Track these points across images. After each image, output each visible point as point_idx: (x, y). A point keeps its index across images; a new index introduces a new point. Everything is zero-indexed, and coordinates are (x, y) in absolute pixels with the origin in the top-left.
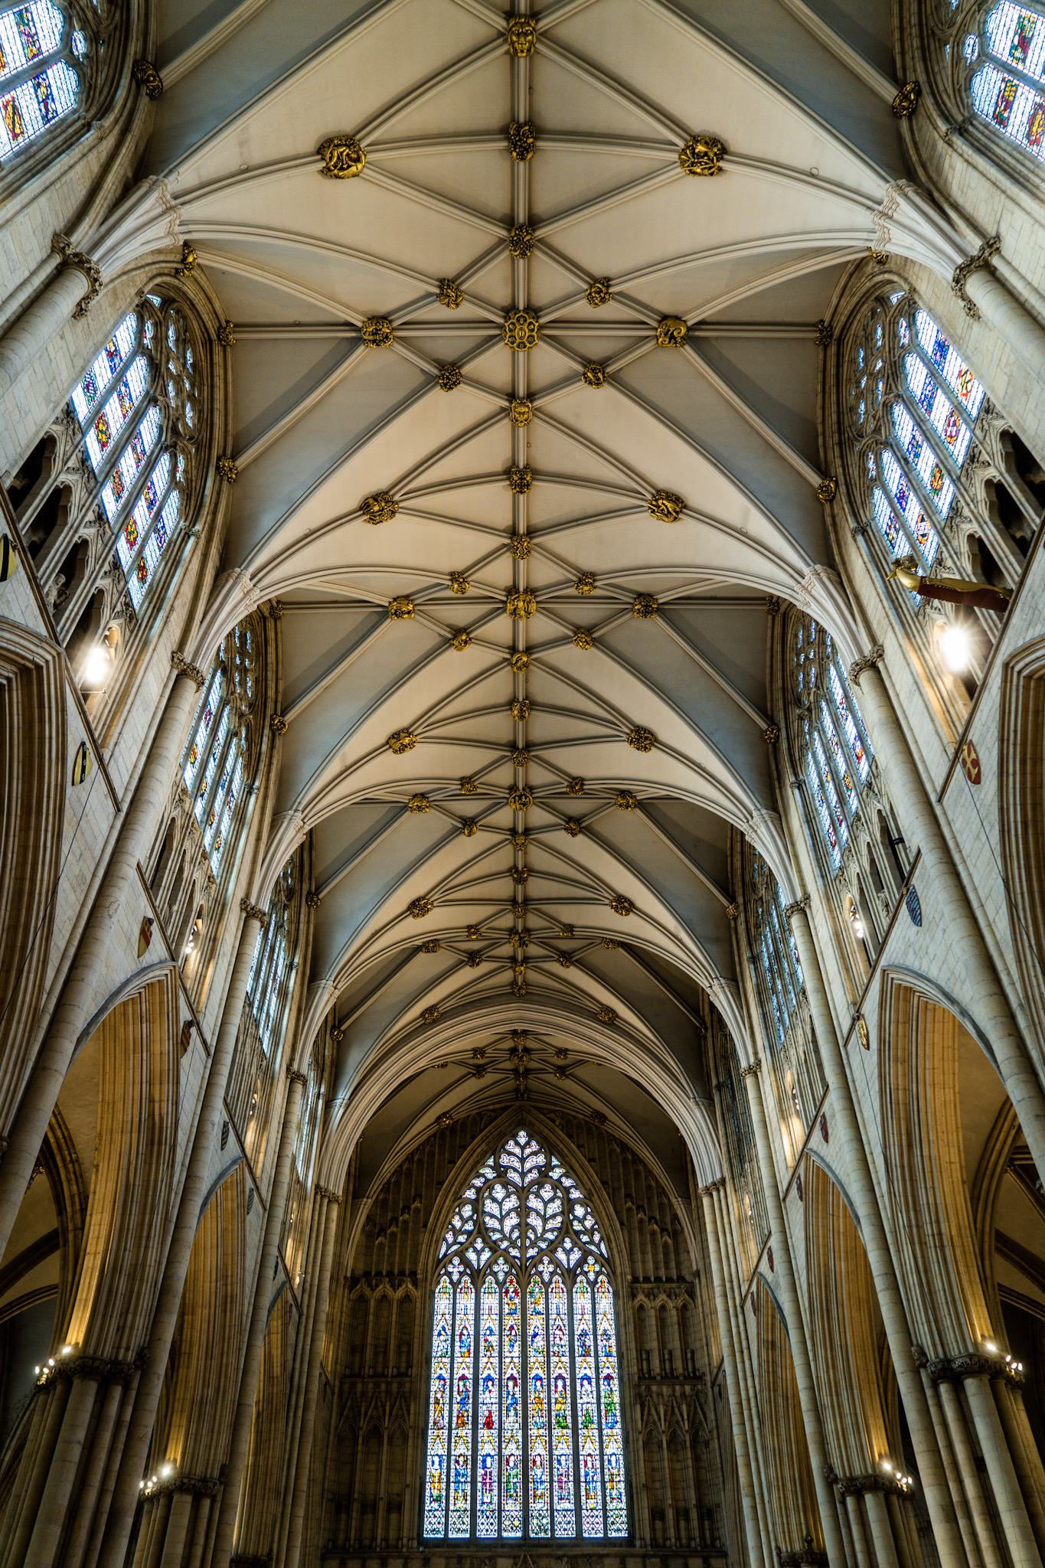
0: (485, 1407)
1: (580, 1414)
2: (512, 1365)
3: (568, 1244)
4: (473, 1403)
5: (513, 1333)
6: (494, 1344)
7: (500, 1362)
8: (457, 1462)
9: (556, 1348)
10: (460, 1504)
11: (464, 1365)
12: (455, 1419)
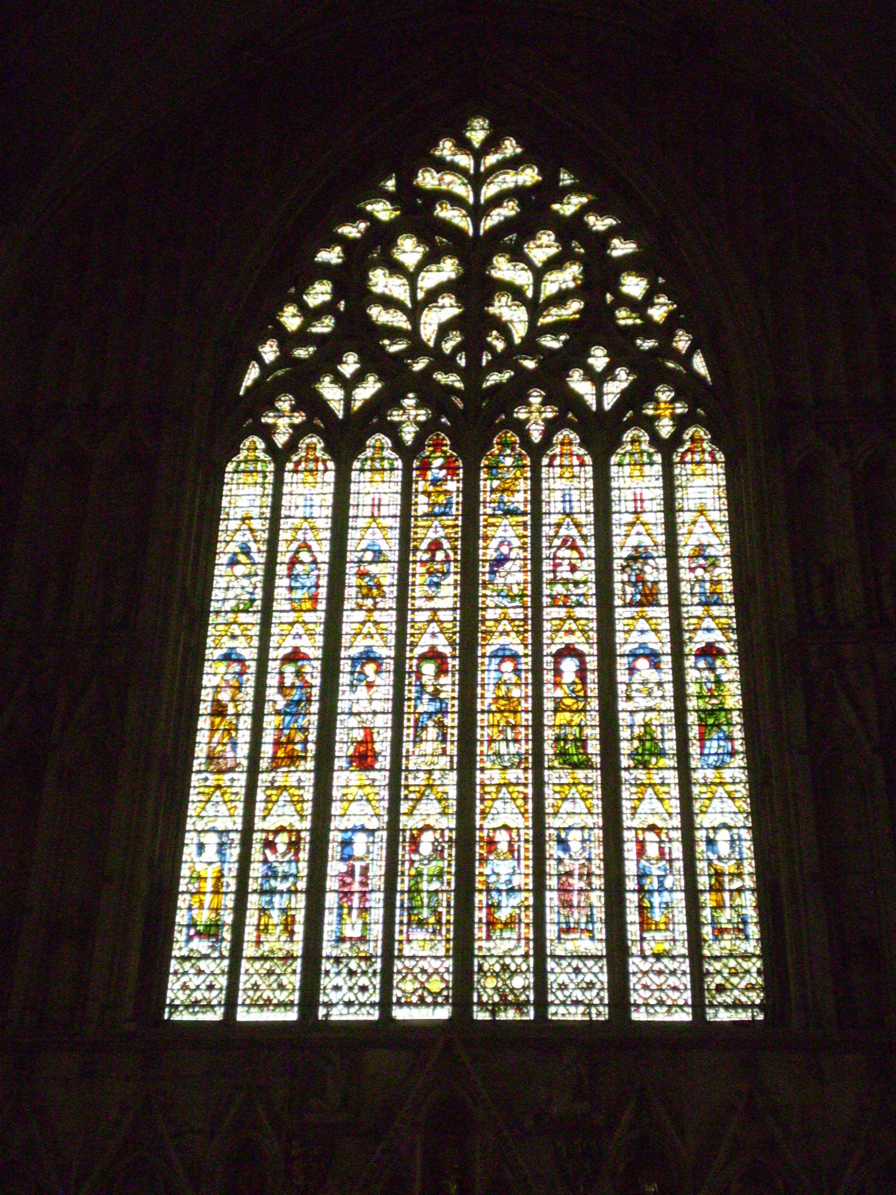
0: (353, 722)
1: (624, 733)
2: (434, 628)
3: (599, 359)
4: (322, 713)
5: (440, 556)
6: (386, 581)
7: (402, 622)
8: (269, 845)
9: (559, 589)
10: (275, 942)
11: (298, 628)
12: (267, 750)
